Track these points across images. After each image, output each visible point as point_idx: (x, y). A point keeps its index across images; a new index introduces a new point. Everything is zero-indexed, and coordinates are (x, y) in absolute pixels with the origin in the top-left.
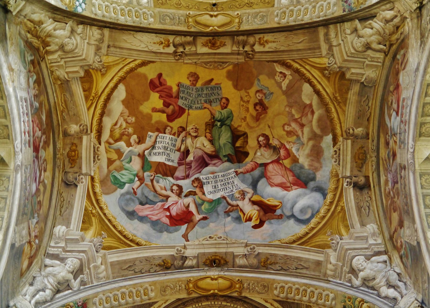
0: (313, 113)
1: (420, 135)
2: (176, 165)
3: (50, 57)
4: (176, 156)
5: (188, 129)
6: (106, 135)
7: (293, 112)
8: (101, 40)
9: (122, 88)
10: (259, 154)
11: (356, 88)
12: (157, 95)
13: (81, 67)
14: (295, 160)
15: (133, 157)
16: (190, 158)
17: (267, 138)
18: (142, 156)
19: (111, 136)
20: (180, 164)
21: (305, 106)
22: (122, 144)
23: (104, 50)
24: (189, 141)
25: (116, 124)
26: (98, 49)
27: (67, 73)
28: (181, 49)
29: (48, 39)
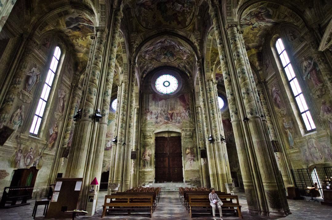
0: (142, 20)
1: (124, 42)
2: (175, 3)
3: (200, 38)
4: (175, 4)
5: (172, 10)
6: (192, 14)
7: (146, 19)
8: (189, 38)
9: (187, 25)
10: (154, 6)
11: (134, 30)
12: (179, 20)
13: (194, 33)
14: (145, 8)
15: (186, 7)
16: (171, 3)
17: (152, 11)
18: (184, 7)
19: (191, 13)
20: (174, 3)
21: (144, 21)
22: (188, 11)
23: (189, 35)
24: (172, 7)
25: (189, 16)
26: (191, 36)
27: (197, 32)
28: (173, 29)
29: (199, 44)
